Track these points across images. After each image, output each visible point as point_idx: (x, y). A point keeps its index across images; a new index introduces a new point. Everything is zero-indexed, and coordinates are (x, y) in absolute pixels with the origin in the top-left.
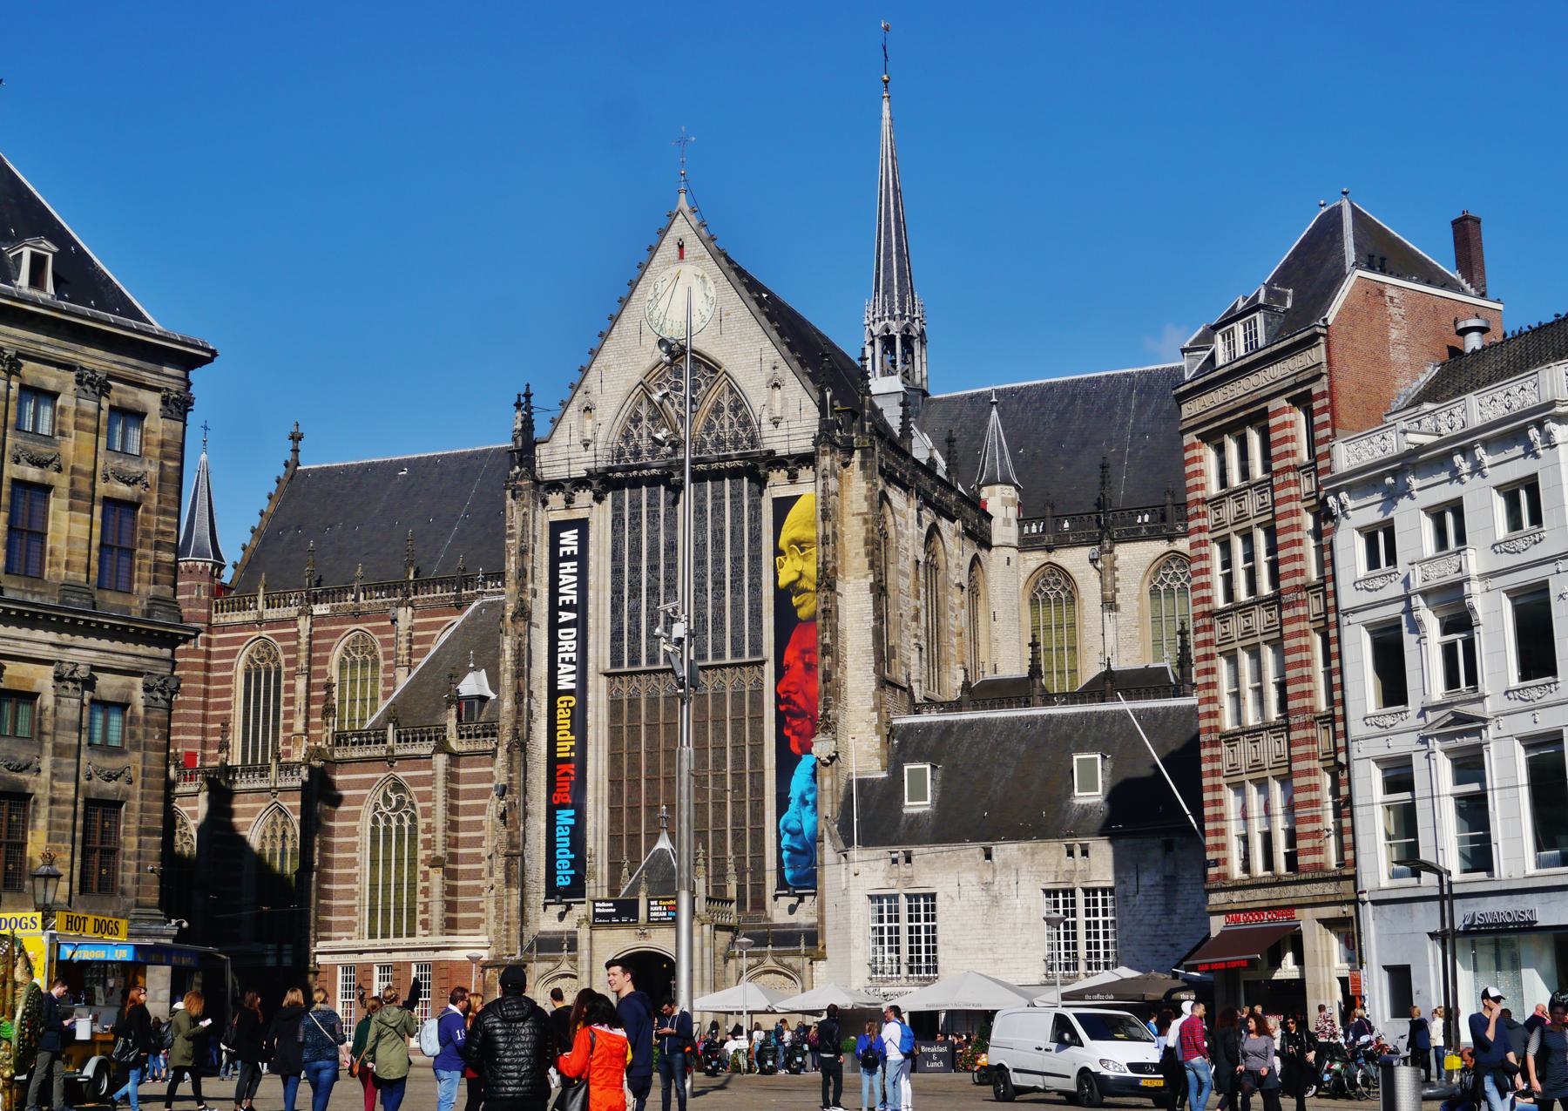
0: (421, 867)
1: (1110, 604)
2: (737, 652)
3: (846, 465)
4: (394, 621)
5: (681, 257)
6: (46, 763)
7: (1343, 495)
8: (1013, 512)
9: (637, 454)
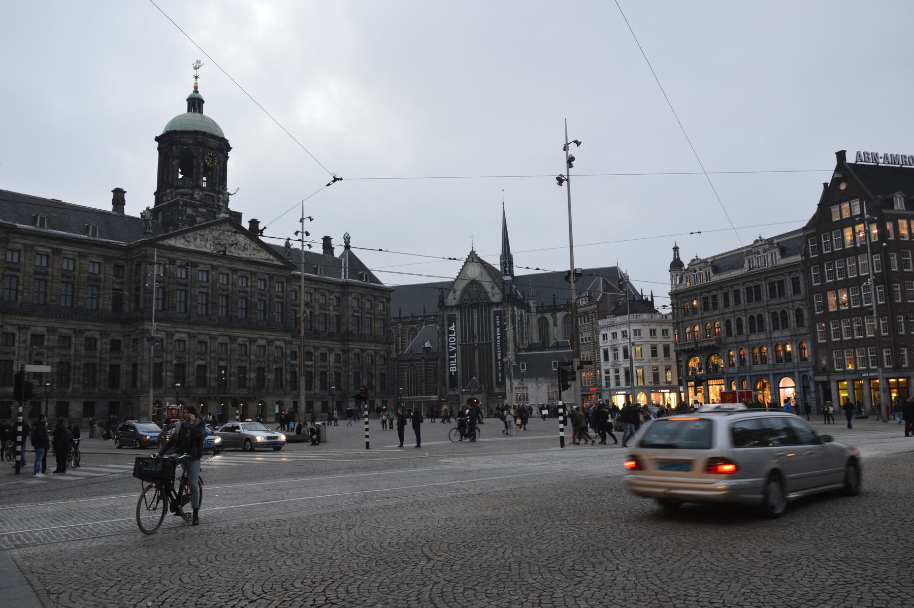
0: (419, 382)
1: (555, 325)
2: (486, 340)
3: (508, 304)
4: (398, 326)
6: (374, 367)
8: (535, 305)
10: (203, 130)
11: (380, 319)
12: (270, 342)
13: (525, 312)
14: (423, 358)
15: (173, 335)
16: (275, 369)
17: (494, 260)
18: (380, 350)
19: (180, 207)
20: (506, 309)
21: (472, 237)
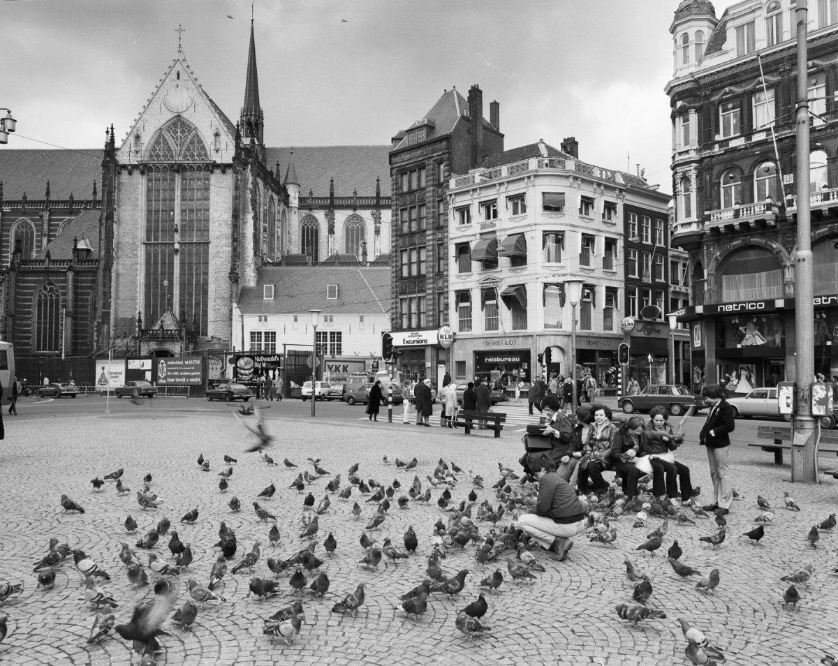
1: (331, 231)
3: (244, 169)
4: (41, 217)
5: (178, 78)
7: (453, 197)
8: (297, 195)
9: (158, 156)
13: (279, 201)
14: (70, 269)
21: (180, 30)
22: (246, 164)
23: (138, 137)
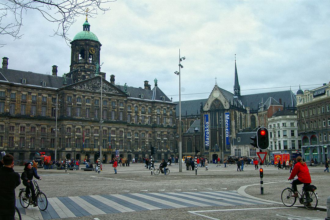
8: (249, 110)
9: (212, 108)
10: (89, 38)
11: (170, 118)
12: (117, 129)
13: (243, 113)
14: (194, 135)
15: (75, 126)
16: (120, 140)
17: (231, 89)
18: (170, 132)
19: (79, 72)
20: (231, 112)
21: (216, 78)
22: (232, 109)
23: (208, 104)
